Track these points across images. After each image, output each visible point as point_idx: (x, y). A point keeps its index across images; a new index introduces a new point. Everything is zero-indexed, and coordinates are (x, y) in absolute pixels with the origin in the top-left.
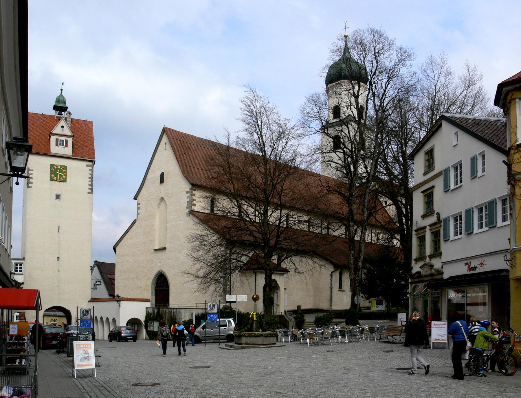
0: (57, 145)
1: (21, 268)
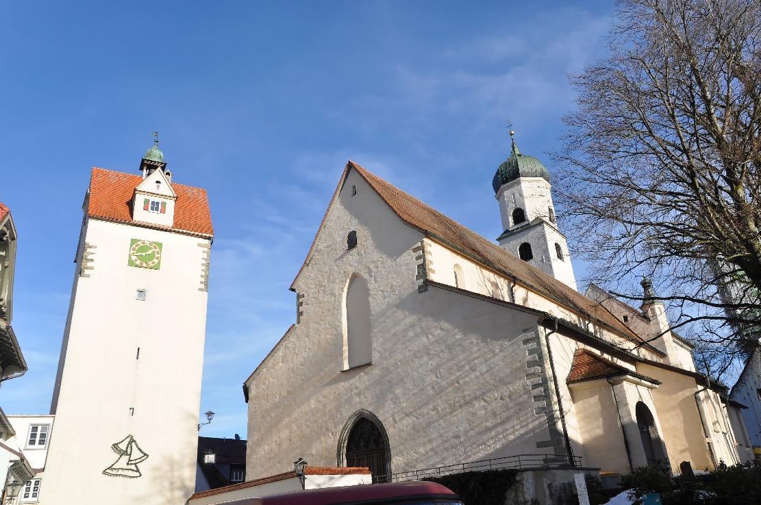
0: (146, 209)
1: (43, 436)
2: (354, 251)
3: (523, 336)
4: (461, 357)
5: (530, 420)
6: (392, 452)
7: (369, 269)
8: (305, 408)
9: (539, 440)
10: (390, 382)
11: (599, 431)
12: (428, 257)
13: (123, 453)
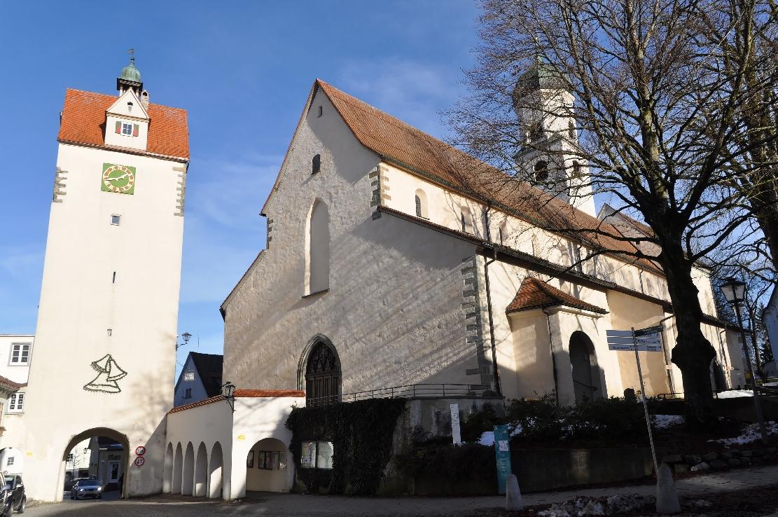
0: (118, 132)
1: (25, 354)
2: (318, 175)
3: (463, 265)
4: (407, 285)
5: (462, 348)
6: (343, 375)
7: (330, 194)
8: (270, 332)
9: (469, 367)
10: (343, 308)
11: (532, 360)
12: (384, 183)
13: (102, 371)
